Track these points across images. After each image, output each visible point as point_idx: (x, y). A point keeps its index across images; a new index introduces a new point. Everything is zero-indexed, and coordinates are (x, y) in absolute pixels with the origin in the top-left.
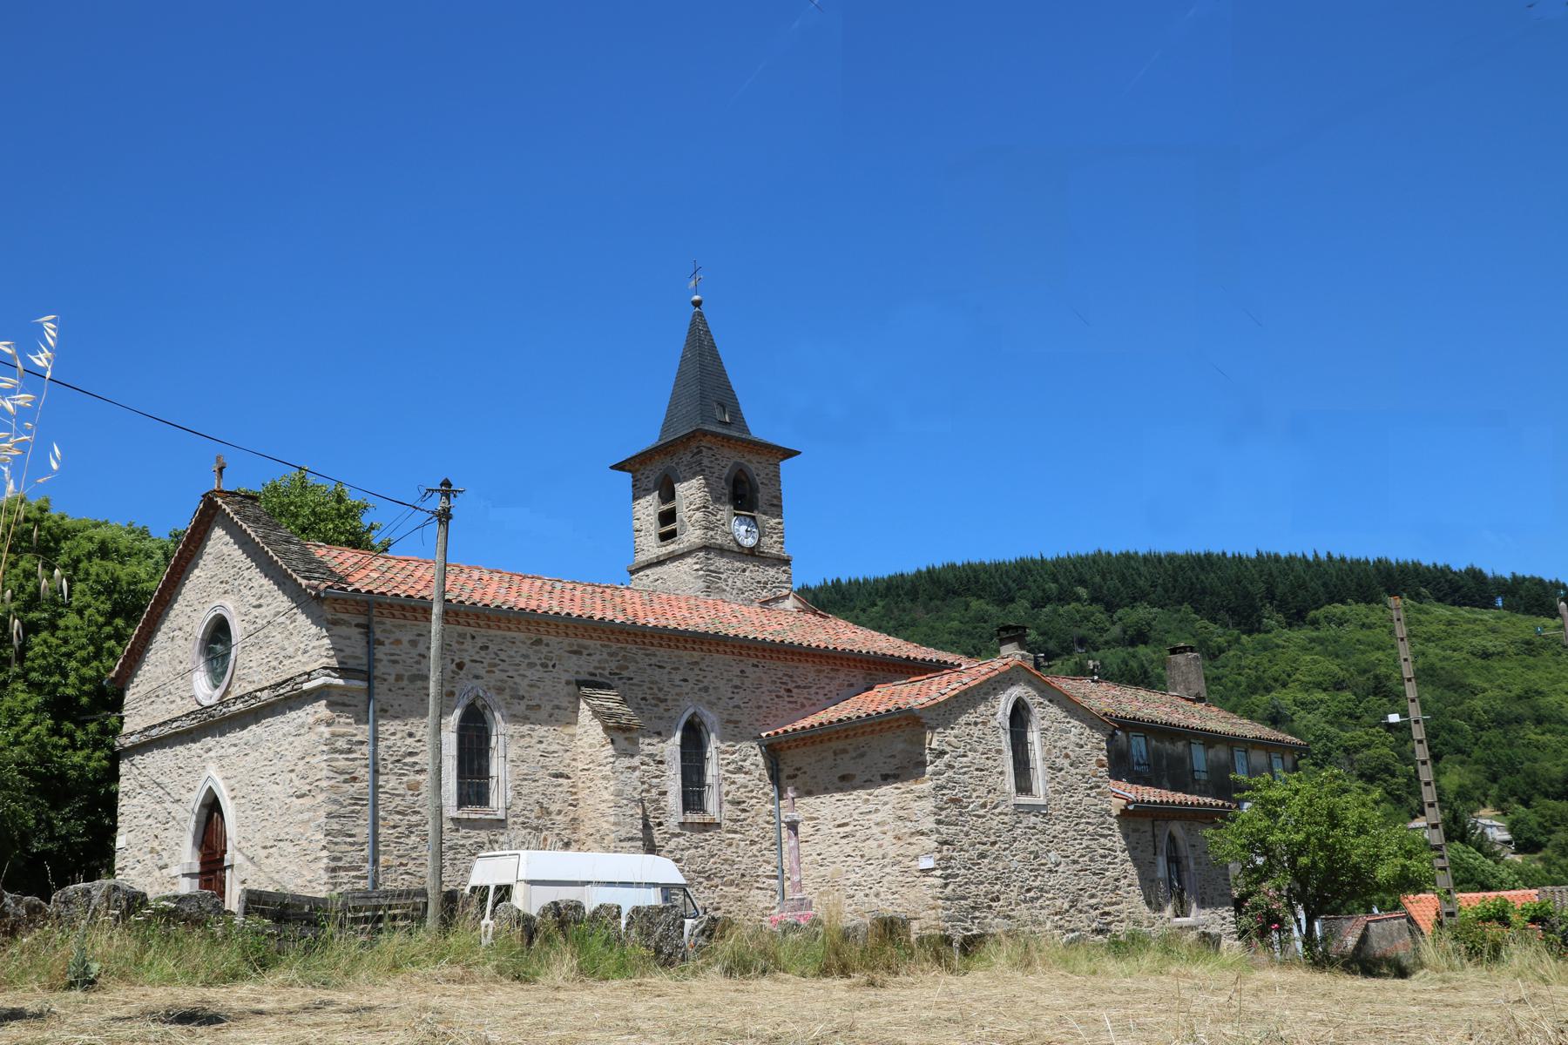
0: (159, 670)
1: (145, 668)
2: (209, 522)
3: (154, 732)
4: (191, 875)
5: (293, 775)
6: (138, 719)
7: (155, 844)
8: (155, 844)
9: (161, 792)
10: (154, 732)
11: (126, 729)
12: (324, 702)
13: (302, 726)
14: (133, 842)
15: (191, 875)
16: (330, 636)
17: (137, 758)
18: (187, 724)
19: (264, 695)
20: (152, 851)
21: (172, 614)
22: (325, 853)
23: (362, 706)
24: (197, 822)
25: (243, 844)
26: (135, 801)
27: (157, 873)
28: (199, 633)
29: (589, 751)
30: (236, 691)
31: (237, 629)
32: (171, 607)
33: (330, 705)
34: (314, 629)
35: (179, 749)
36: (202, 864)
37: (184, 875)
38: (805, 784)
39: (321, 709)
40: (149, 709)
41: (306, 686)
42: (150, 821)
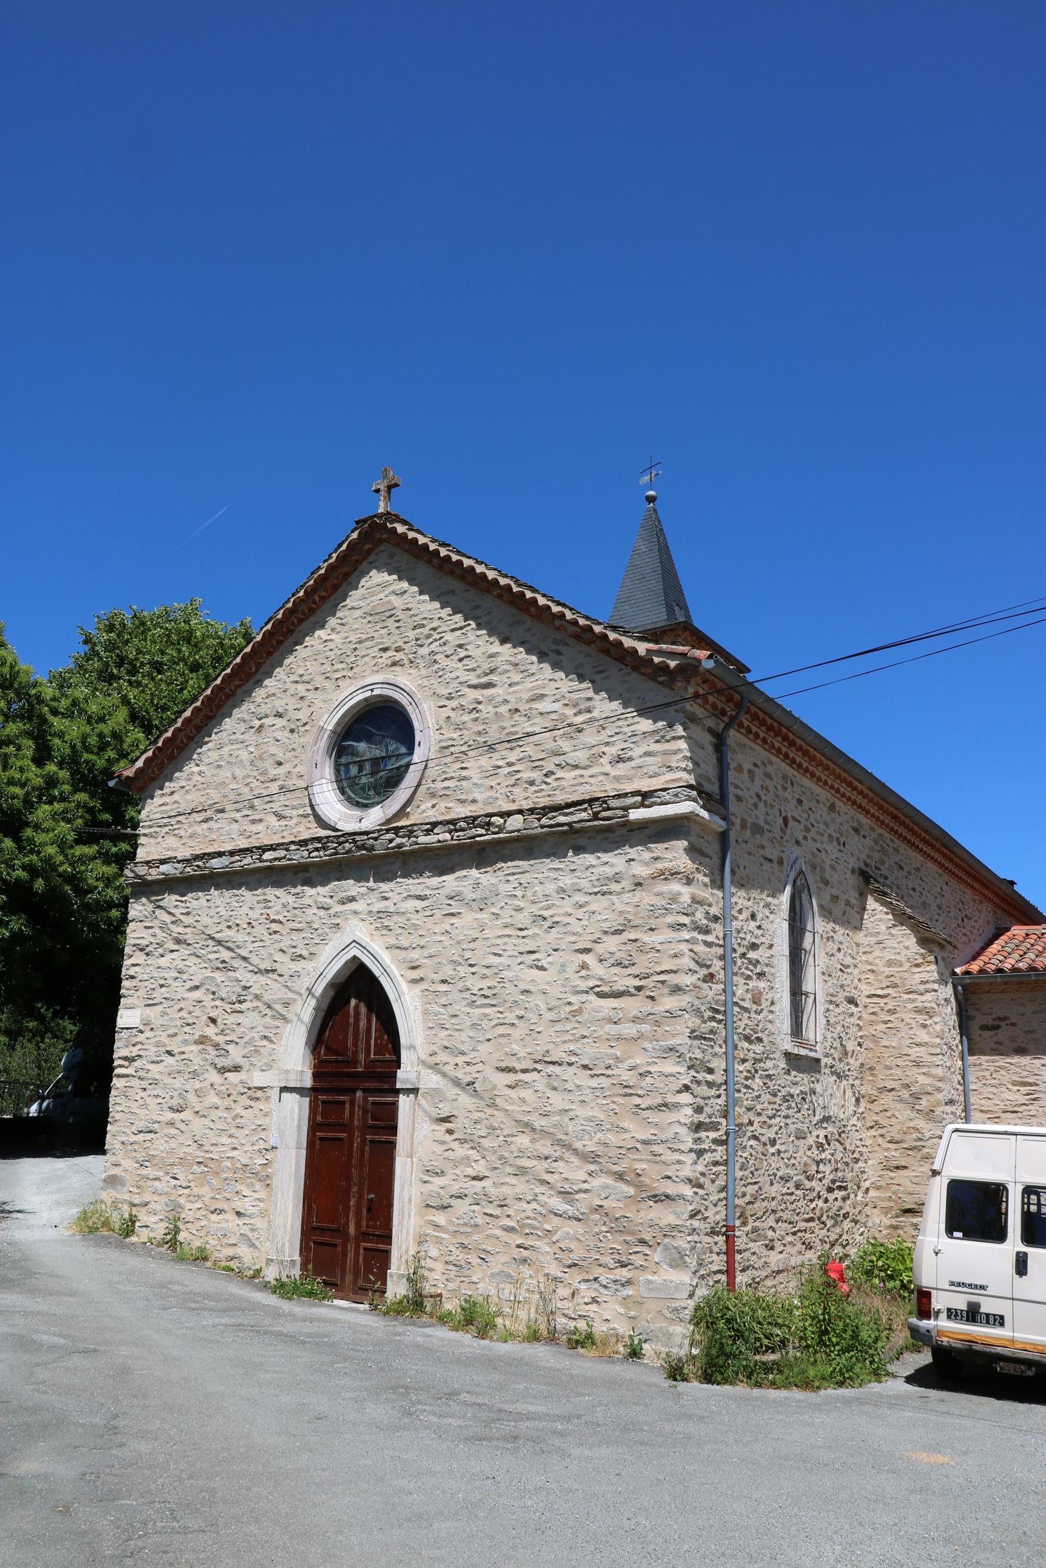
0: (225, 774)
1: (190, 768)
2: (358, 562)
3: (216, 863)
4: (300, 1091)
5: (589, 959)
6: (171, 841)
7: (211, 1031)
8: (211, 1031)
9: (226, 955)
10: (216, 863)
11: (141, 854)
12: (686, 843)
13: (616, 878)
14: (157, 1022)
15: (300, 1091)
16: (688, 739)
17: (170, 900)
18: (299, 856)
19: (515, 822)
20: (202, 1040)
21: (259, 694)
22: (686, 1098)
23: (716, 861)
24: (317, 1009)
25: (442, 1057)
26: (163, 962)
27: (213, 1076)
28: (330, 722)
29: (887, 971)
30: (424, 812)
31: (427, 721)
32: (259, 683)
33: (693, 851)
34: (645, 725)
35: (271, 893)
36: (316, 1076)
37: (284, 1089)
38: (1013, 1039)
39: (675, 854)
40: (198, 829)
41: (635, 815)
42: (196, 995)
